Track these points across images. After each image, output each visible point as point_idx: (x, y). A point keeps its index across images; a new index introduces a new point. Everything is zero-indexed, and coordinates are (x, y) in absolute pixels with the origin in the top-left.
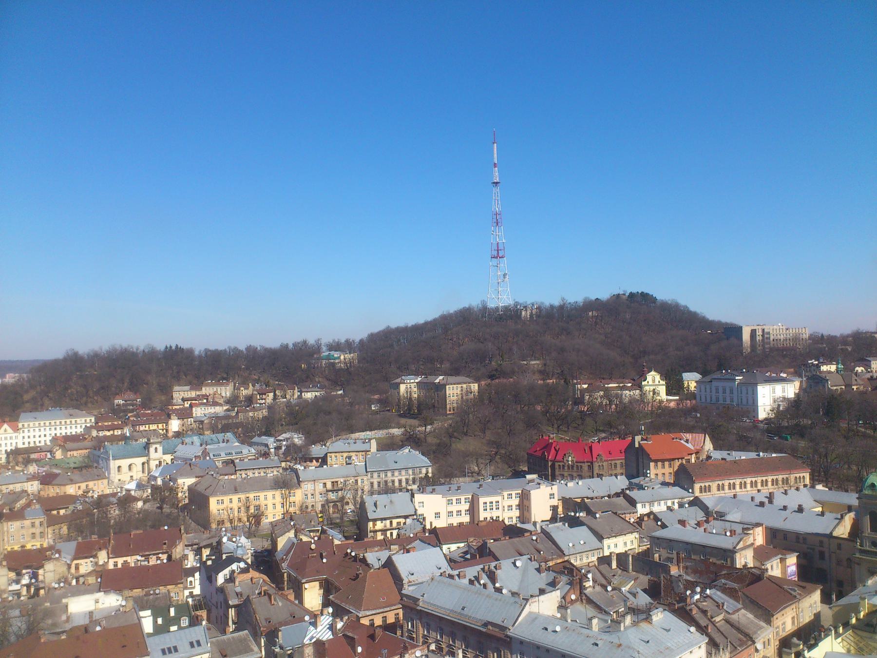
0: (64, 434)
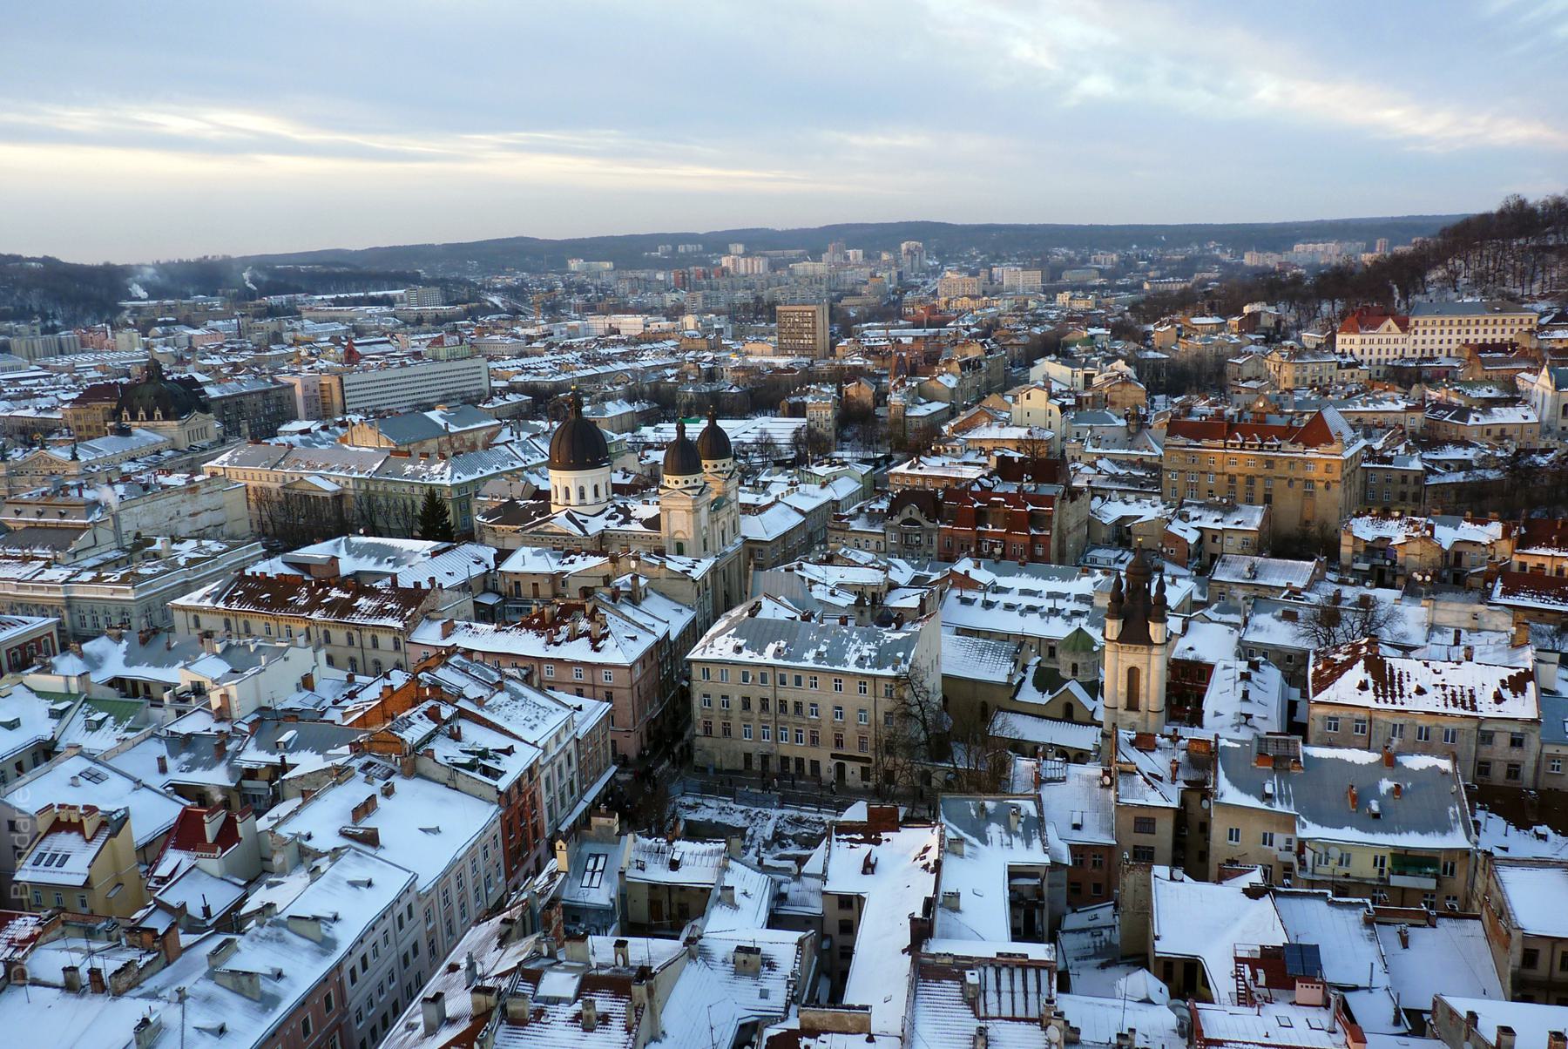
0: (1480, 341)
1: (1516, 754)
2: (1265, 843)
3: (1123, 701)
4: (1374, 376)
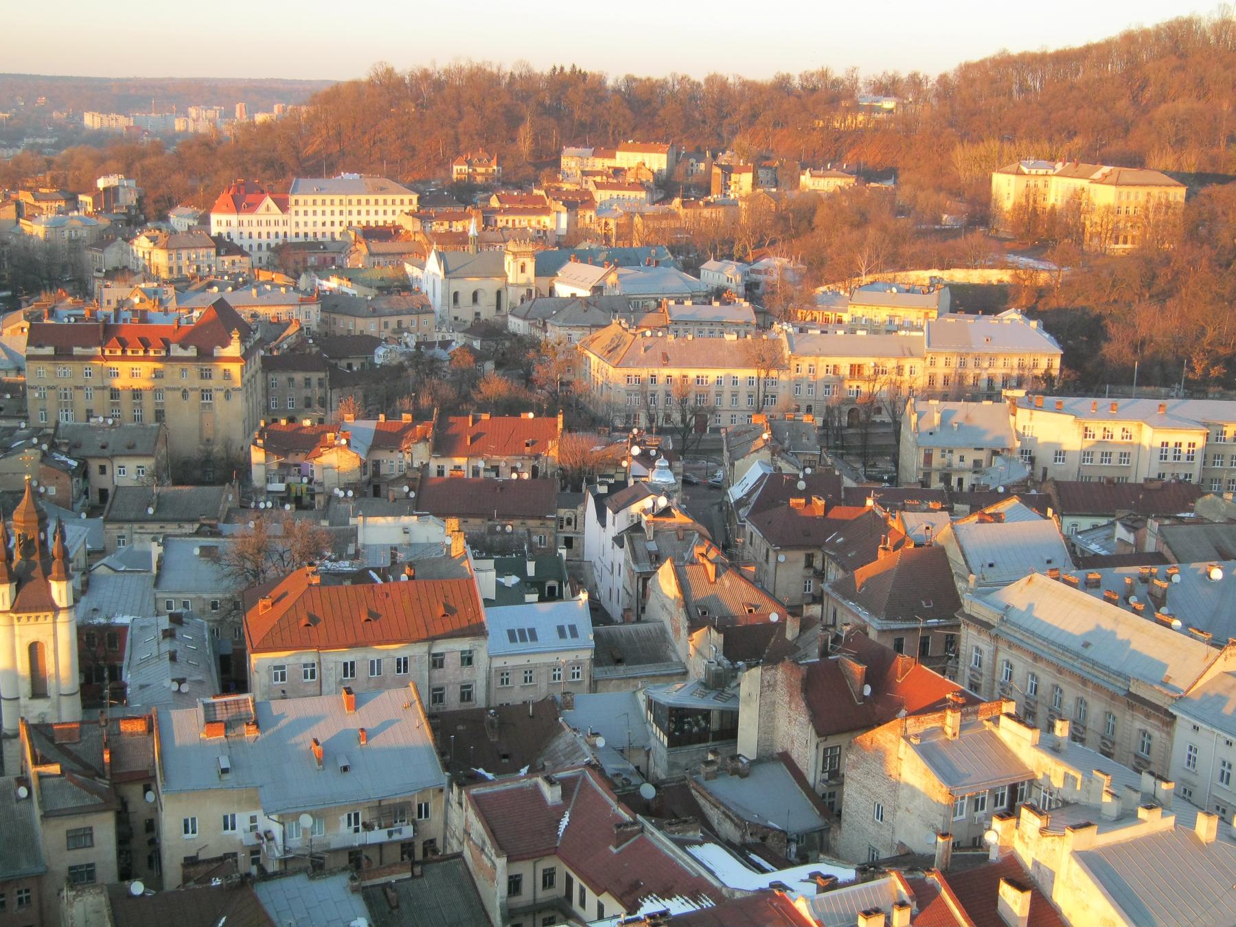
1: (466, 674)
2: (226, 828)
3: (25, 688)
4: (256, 263)
